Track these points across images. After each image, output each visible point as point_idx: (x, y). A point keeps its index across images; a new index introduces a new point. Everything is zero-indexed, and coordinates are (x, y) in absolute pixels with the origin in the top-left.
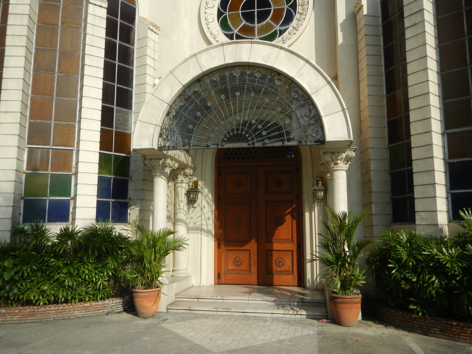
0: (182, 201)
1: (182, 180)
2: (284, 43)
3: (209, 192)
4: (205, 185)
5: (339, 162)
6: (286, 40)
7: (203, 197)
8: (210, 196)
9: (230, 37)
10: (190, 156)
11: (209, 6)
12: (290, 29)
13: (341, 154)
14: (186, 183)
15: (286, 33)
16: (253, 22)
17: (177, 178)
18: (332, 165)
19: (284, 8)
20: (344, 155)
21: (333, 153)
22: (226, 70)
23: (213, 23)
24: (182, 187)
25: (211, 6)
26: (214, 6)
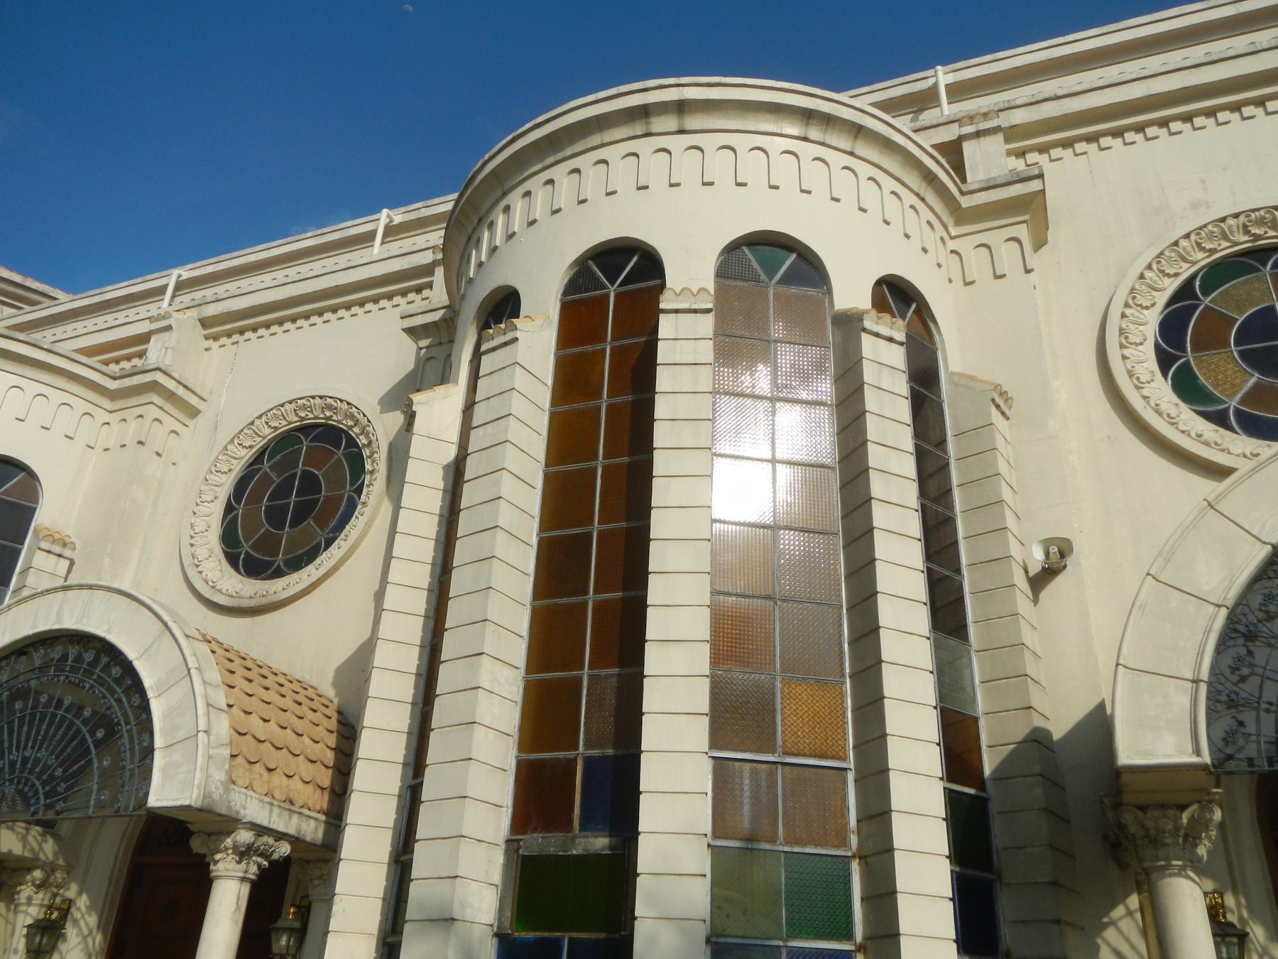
0: (16, 951)
1: (30, 899)
2: (317, 569)
3: (99, 927)
4: (90, 908)
5: (218, 856)
6: (322, 562)
7: (79, 939)
8: (99, 938)
9: (232, 559)
10: (57, 838)
11: (204, 497)
12: (342, 536)
13: (222, 837)
14: (41, 906)
15: (331, 549)
16: (283, 528)
17: (19, 893)
18: (212, 867)
19: (342, 497)
20: (229, 842)
21: (209, 835)
22: (43, 645)
23: (206, 534)
24: (26, 913)
25: (209, 498)
26: (216, 498)
